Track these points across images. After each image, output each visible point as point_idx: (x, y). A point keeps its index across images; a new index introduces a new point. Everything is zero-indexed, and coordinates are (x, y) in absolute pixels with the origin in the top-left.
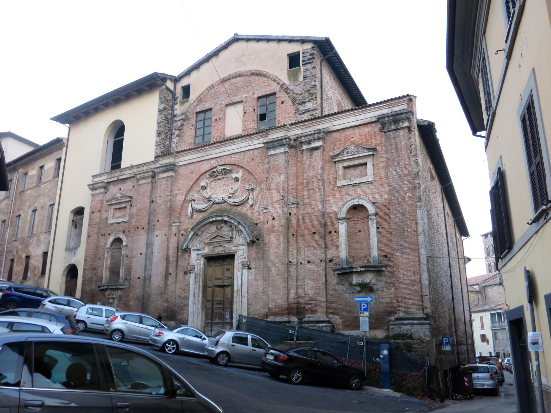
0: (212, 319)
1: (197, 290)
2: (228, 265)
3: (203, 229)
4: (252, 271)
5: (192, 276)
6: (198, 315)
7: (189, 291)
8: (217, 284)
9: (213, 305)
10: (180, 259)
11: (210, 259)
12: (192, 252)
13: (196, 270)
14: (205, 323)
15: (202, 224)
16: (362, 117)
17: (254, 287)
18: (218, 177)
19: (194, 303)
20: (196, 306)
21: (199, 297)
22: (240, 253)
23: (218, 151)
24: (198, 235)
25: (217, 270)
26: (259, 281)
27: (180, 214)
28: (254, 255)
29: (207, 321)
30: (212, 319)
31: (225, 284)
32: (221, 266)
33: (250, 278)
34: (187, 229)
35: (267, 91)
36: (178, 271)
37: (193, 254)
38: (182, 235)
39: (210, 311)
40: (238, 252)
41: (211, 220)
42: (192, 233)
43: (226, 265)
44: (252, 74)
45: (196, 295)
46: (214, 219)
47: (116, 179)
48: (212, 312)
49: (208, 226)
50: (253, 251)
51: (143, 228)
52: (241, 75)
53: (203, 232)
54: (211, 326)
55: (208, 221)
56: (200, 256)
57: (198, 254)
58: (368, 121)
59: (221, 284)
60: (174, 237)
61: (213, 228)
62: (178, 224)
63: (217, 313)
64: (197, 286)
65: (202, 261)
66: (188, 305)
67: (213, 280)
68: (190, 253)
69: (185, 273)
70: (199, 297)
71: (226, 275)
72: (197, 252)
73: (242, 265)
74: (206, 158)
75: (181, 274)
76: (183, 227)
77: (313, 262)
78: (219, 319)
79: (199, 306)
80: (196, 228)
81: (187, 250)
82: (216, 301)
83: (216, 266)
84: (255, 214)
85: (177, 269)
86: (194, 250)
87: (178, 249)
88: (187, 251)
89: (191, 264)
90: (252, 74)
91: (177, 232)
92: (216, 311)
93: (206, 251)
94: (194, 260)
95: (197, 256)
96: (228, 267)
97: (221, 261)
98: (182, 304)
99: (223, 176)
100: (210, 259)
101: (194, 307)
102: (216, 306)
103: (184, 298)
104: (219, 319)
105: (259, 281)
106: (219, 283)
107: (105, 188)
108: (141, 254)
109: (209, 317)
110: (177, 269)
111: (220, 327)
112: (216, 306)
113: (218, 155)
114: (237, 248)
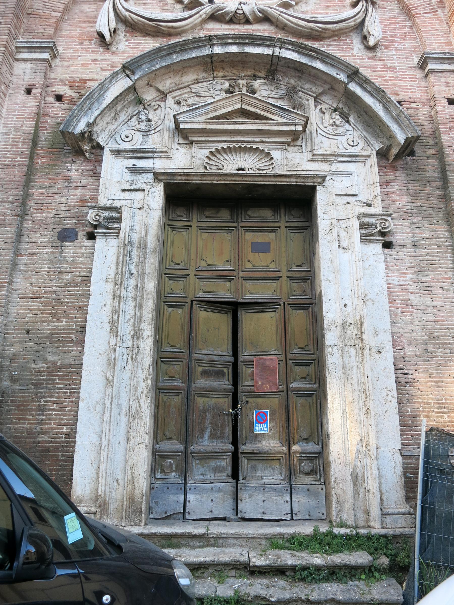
0: (187, 440)
1: (129, 308)
2: (260, 229)
3: (166, 84)
4: (403, 256)
5: (106, 250)
6: (133, 417)
7: (83, 310)
8: (210, 296)
9: (189, 379)
10: (40, 179)
11: (186, 198)
12: (107, 157)
13: (125, 225)
14: (155, 452)
15: (176, 58)
17: (417, 315)
19: (112, 364)
20: (123, 378)
21: (137, 335)
24: (140, 101)
25: (213, 246)
26: (438, 292)
27: (57, 28)
28: (402, 202)
29: (163, 446)
30: (187, 440)
31: (249, 297)
32: (229, 230)
33: (396, 280)
34: (84, 81)
36: (28, 225)
37: (113, 170)
38: (59, 98)
39: (175, 400)
40: (328, 183)
41: (217, 50)
42: (123, 83)
43: (249, 230)
45: (126, 330)
46: (233, 49)
48: (188, 407)
49: (190, 77)
50: (396, 187)
53: (163, 96)
54: (185, 471)
55: (206, 51)
56: (151, 176)
57: (134, 171)
59: (228, 297)
60: (21, 96)
61: (213, 94)
62: (46, 55)
63: (204, 411)
64: (128, 293)
65: (156, 197)
66: (76, 370)
67: (192, 278)
68: (99, 161)
69: (66, 236)
70: (137, 335)
71: (249, 266)
72: (130, 163)
73: (362, 226)
75: (40, 242)
76: (62, 72)
78: (212, 436)
79: (138, 378)
80: (146, 68)
81: (82, 148)
82: (201, 362)
83: (203, 229)
84: (388, 75)
85: (22, 216)
86: (117, 153)
87: (35, 142)
88: (79, 152)
89: (103, 201)
91: (38, 81)
92: (201, 402)
93: (183, 160)
94: (116, 189)
95: (128, 176)
96: (261, 238)
97: (225, 213)
98: (40, 365)
100: (186, 198)
101: (109, 382)
102: (200, 383)
103: (54, 337)
104: (212, 436)
105: (438, 292)
106: (224, 292)
109: (173, 427)
110: (22, 216)
111: (217, 470)
112: (200, 383)
114: (325, 167)
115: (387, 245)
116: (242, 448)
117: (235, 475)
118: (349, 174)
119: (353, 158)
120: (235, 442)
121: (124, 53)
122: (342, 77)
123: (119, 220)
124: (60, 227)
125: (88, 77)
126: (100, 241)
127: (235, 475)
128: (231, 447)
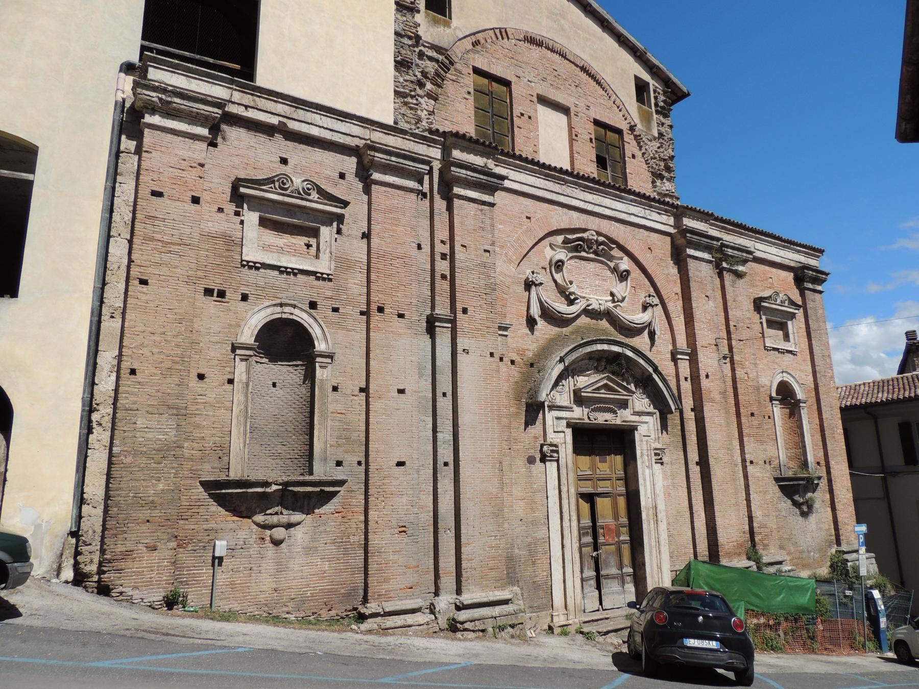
4: (667, 468)
16: (782, 253)
18: (583, 254)
22: (642, 430)
23: (589, 197)
31: (600, 490)
34: (524, 350)
35: (610, 119)
38: (513, 362)
44: (583, 69)
47: (275, 120)
51: (401, 316)
52: (563, 56)
56: (564, 422)
58: (787, 262)
69: (531, 460)
74: (562, 199)
77: (757, 464)
90: (583, 69)
99: (592, 256)
103: (534, 523)
107: (215, 129)
108: (401, 391)
113: (590, 207)
115: (662, 464)
116: (603, 573)
117: (599, 588)
118: (646, 423)
119: (649, 414)
120: (597, 570)
121: (542, 330)
122: (651, 370)
123: (557, 452)
124: (528, 455)
125: (525, 347)
126: (547, 463)
127: (599, 588)
128: (595, 573)
